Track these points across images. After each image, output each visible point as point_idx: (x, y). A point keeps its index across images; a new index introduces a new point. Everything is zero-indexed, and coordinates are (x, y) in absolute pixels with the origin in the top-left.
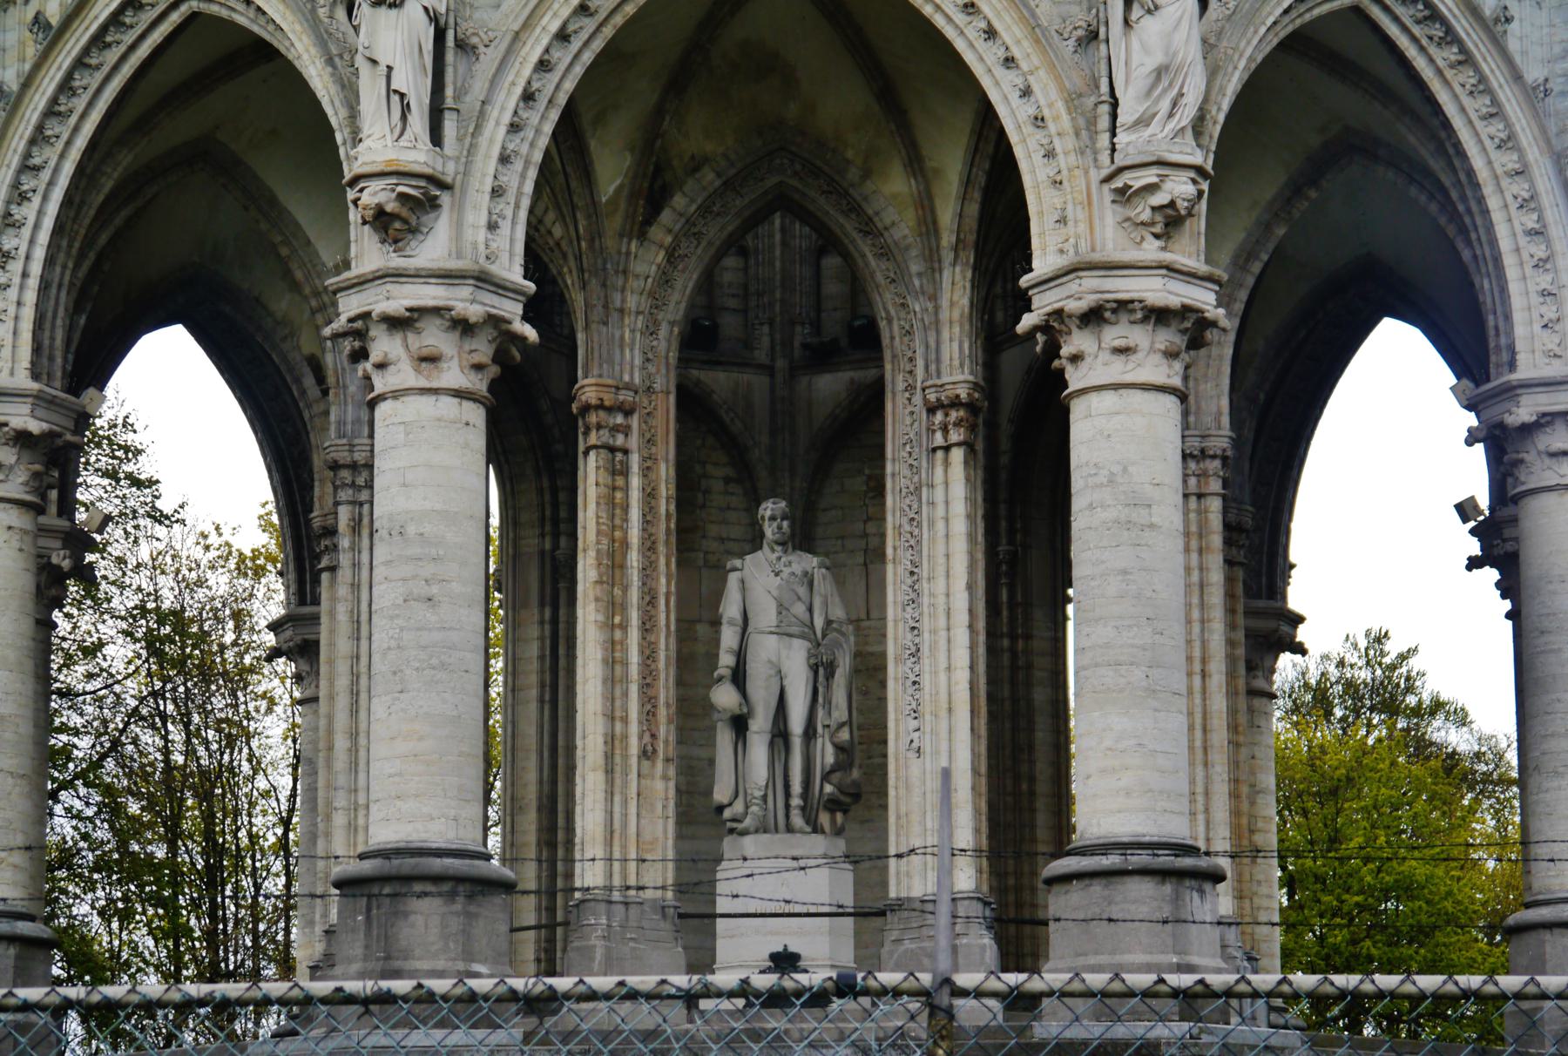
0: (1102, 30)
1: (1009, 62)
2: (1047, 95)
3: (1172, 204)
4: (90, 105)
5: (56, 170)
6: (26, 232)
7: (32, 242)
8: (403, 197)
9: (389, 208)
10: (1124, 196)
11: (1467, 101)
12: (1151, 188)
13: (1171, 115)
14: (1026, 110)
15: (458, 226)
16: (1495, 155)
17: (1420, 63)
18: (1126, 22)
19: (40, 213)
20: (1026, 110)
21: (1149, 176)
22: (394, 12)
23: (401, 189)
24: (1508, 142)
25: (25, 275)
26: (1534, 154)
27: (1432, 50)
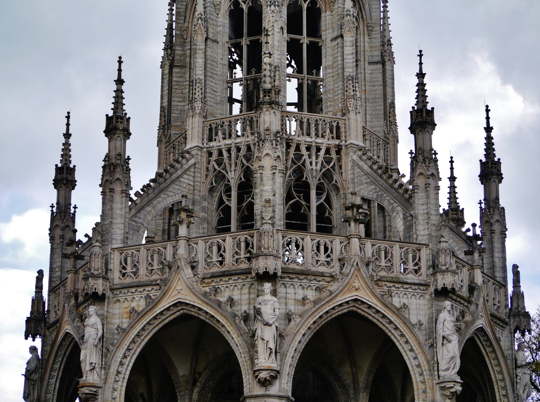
0: (435, 345)
1: (412, 350)
2: (422, 359)
3: (456, 392)
4: (148, 334)
5: (136, 351)
6: (125, 367)
7: (126, 369)
8: (271, 376)
9: (268, 378)
10: (443, 388)
11: (492, 361)
12: (452, 387)
13: (453, 368)
14: (415, 363)
15: (280, 383)
16: (497, 375)
17: (483, 351)
18: (443, 344)
19: (130, 362)
20: (415, 363)
21: (451, 385)
22: (269, 327)
23: (272, 374)
24: (501, 372)
25: (124, 378)
26: (506, 376)
27: (486, 348)
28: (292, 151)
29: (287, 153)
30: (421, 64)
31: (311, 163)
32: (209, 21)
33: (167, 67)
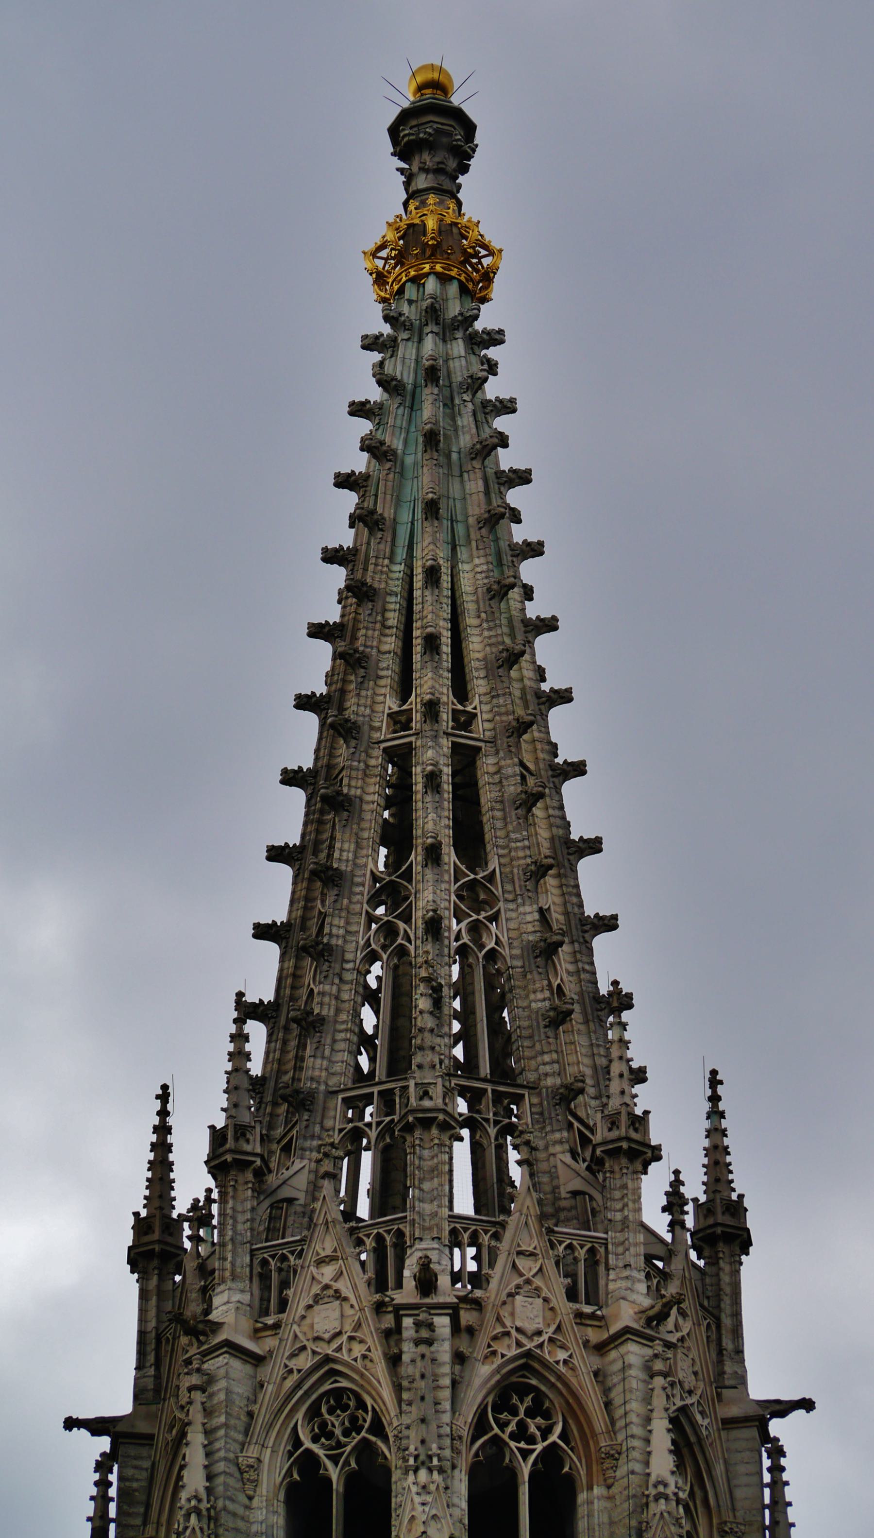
32: (224, 1518)
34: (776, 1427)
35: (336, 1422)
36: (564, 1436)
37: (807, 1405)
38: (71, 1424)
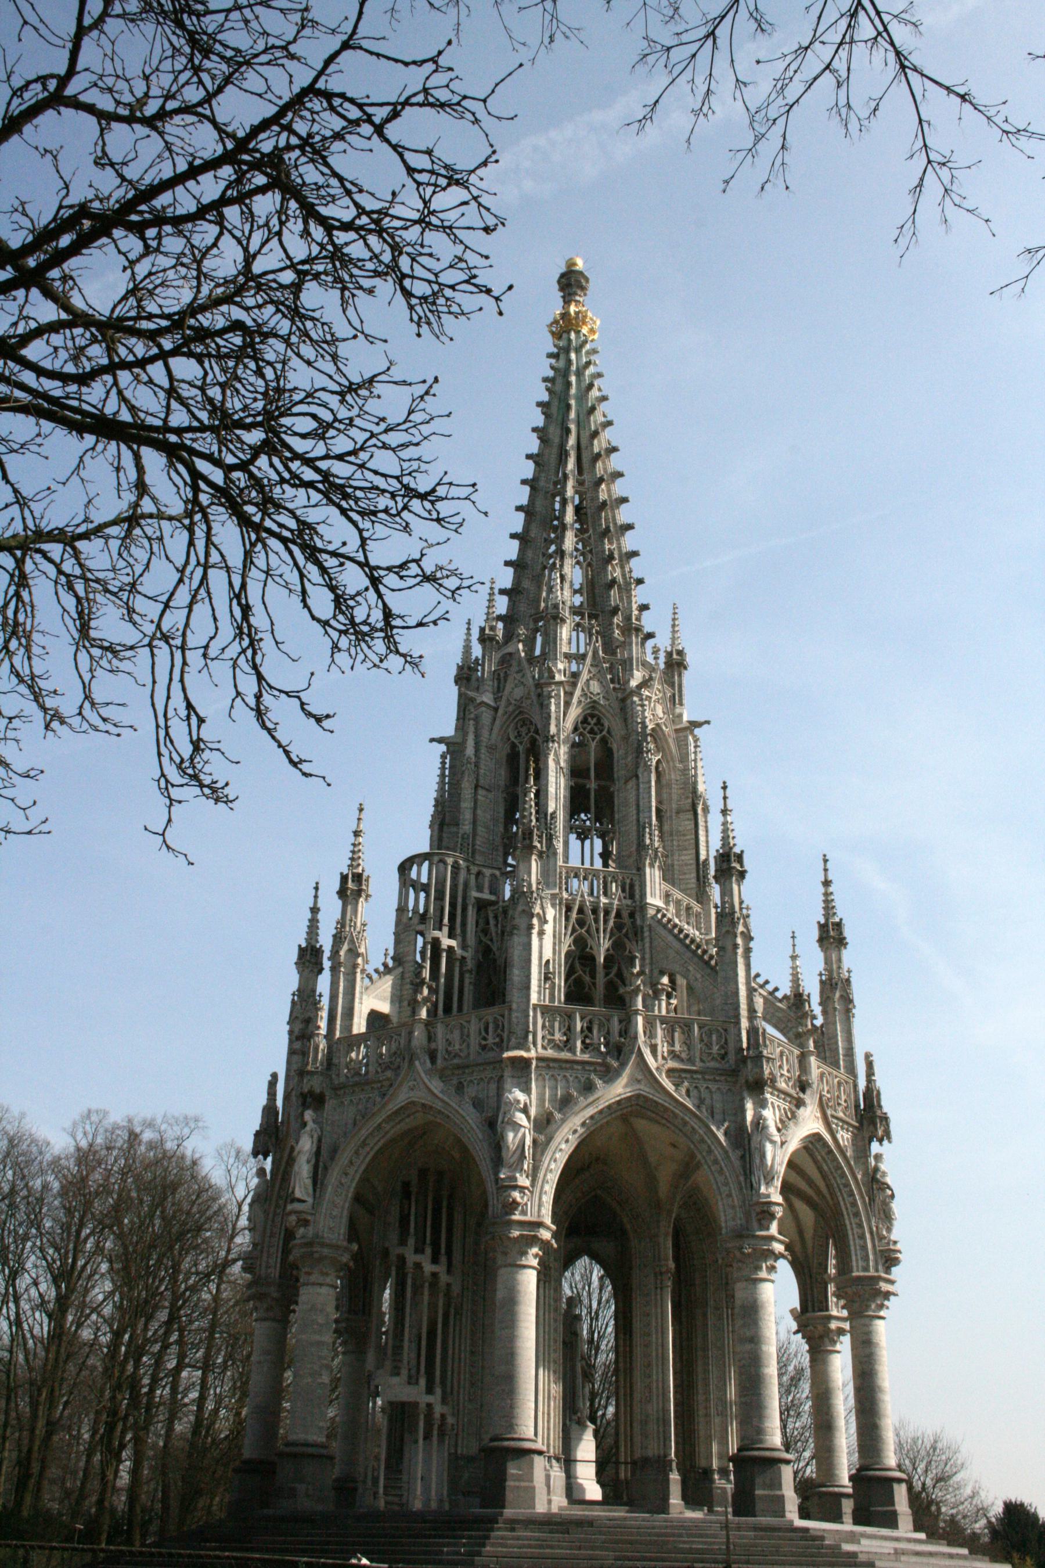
28: (574, 915)
29: (567, 918)
30: (725, 798)
31: (598, 930)
33: (436, 827)
34: (697, 731)
35: (524, 730)
36: (609, 732)
37: (708, 722)
38: (432, 740)
